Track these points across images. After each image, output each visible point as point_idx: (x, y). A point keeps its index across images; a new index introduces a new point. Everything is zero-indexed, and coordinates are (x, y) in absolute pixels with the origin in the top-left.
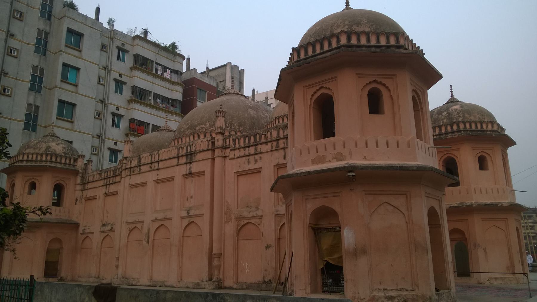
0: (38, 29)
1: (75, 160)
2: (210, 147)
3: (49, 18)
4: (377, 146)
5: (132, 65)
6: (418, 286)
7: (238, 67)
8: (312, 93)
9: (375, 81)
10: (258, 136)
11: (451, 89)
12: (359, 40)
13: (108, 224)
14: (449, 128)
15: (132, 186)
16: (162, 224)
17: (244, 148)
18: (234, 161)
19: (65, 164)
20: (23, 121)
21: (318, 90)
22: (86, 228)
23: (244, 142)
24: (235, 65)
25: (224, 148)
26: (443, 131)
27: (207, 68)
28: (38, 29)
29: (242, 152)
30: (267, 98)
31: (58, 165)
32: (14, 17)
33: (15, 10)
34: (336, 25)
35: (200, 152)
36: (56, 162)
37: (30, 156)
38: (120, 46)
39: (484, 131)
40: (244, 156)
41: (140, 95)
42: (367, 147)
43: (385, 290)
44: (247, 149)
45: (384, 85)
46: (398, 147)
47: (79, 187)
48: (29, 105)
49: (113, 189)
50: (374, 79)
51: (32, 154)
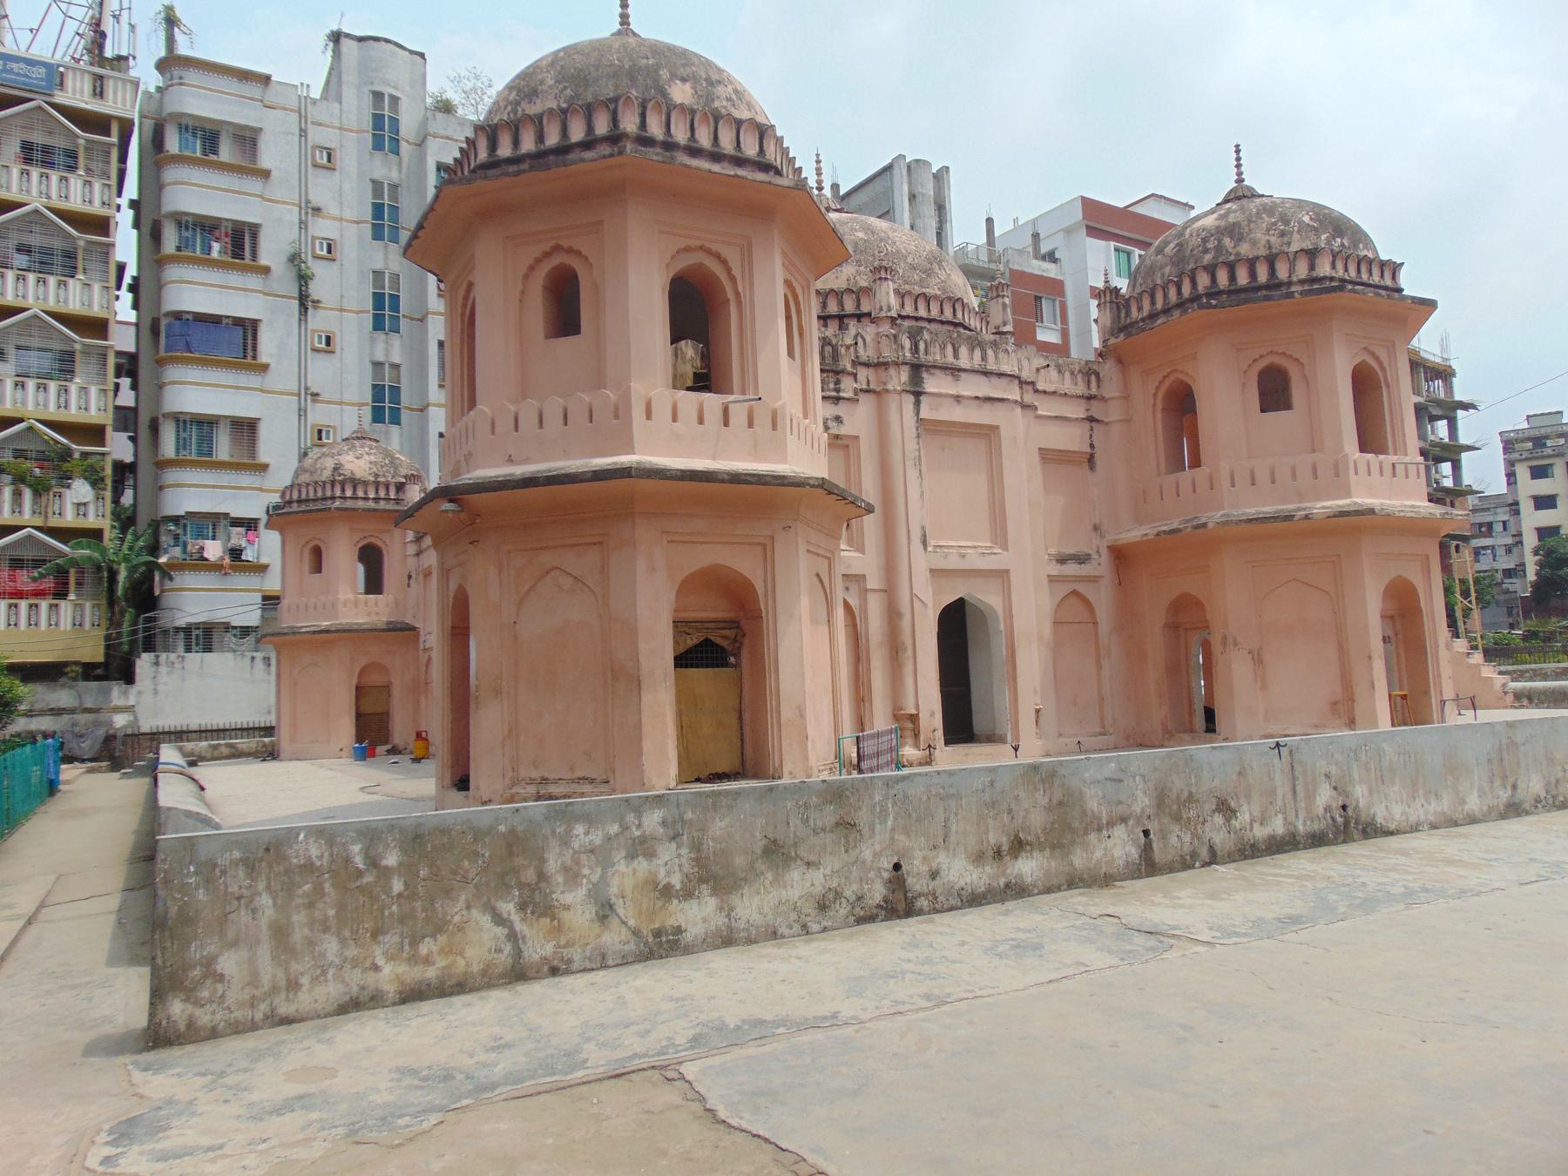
0: (373, 181)
1: (400, 487)
7: (926, 164)
9: (558, 248)
11: (1238, 159)
14: (1172, 292)
19: (377, 500)
24: (917, 161)
26: (1159, 305)
28: (373, 181)
30: (1036, 236)
31: (361, 504)
32: (315, 166)
33: (315, 147)
36: (355, 498)
37: (304, 491)
39: (1279, 285)
45: (579, 253)
47: (412, 549)
48: (377, 365)
50: (552, 243)
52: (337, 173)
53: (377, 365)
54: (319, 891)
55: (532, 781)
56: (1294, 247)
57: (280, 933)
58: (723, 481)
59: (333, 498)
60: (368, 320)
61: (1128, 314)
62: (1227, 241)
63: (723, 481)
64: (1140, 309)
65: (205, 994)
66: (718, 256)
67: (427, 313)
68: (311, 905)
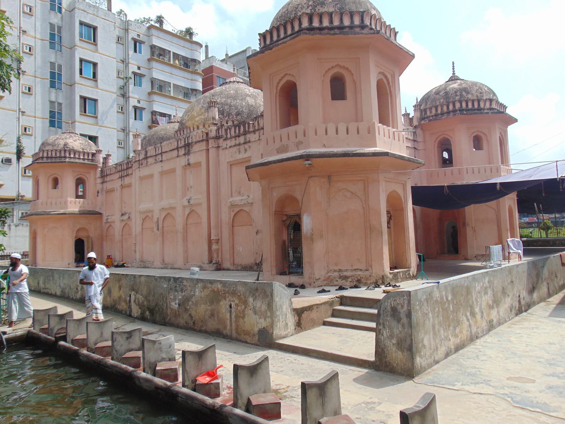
0: (51, 24)
2: (205, 138)
3: (60, 12)
4: (337, 133)
5: (149, 57)
6: (372, 267)
8: (278, 81)
10: (247, 125)
11: (453, 67)
12: (321, 22)
13: (126, 214)
15: (141, 179)
16: (168, 214)
17: (235, 137)
18: (226, 151)
19: (84, 159)
20: (47, 119)
21: (283, 78)
22: (109, 217)
23: (235, 132)
25: (217, 138)
26: (439, 112)
27: (227, 55)
29: (232, 142)
31: (77, 161)
34: (300, 6)
35: (196, 143)
36: (75, 158)
37: (50, 153)
38: (136, 37)
39: (481, 109)
40: (235, 146)
41: (159, 88)
42: (326, 134)
43: (340, 270)
44: (237, 138)
45: (347, 69)
46: (358, 133)
47: (99, 181)
48: (52, 103)
49: (127, 180)
51: (52, 151)
52: (34, 17)
53: (52, 103)
54: (439, 309)
55: (335, 271)
56: (484, 98)
57: (434, 327)
58: (406, 160)
59: (65, 157)
60: (48, 82)
61: (426, 113)
62: (464, 93)
63: (406, 160)
64: (431, 112)
65: (422, 354)
66: (386, 77)
67: (75, 83)
68: (438, 316)
